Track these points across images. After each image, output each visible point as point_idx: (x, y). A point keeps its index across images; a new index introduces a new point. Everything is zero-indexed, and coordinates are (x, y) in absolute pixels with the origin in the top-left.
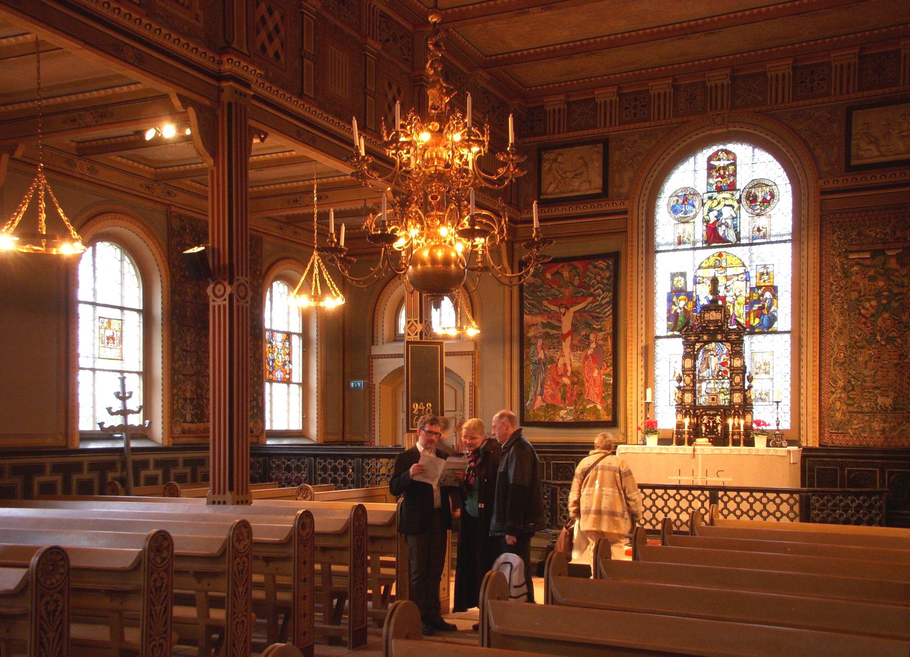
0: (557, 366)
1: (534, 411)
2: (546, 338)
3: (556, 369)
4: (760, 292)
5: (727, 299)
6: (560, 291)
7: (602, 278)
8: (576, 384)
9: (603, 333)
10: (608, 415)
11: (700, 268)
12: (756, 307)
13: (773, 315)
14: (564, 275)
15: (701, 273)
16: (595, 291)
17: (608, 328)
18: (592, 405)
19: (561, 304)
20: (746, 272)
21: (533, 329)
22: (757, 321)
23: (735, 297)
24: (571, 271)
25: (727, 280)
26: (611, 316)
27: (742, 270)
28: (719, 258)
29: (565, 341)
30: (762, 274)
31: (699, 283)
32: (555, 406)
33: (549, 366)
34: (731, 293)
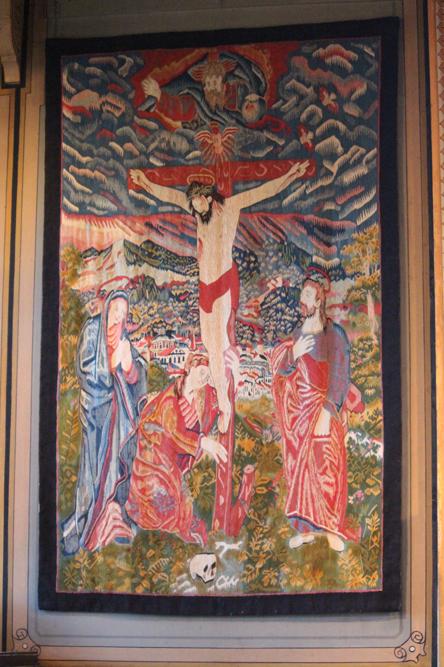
0: (179, 396)
1: (92, 557)
2: (142, 296)
3: (177, 407)
6: (190, 141)
7: (341, 101)
8: (252, 460)
9: (349, 283)
10: (368, 572)
14: (208, 88)
16: (315, 141)
17: (365, 269)
18: (310, 538)
19: (196, 184)
21: (92, 265)
24: (231, 74)
26: (376, 227)
29: (209, 310)
32: (171, 538)
33: (151, 398)
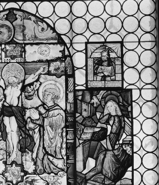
4: (95, 100)
5: (28, 114)
12: (87, 134)
13: (124, 151)
20: (65, 57)
22: (91, 163)
23: (43, 111)
27: (55, 51)
28: (8, 23)
30: (99, 62)
34: (36, 102)
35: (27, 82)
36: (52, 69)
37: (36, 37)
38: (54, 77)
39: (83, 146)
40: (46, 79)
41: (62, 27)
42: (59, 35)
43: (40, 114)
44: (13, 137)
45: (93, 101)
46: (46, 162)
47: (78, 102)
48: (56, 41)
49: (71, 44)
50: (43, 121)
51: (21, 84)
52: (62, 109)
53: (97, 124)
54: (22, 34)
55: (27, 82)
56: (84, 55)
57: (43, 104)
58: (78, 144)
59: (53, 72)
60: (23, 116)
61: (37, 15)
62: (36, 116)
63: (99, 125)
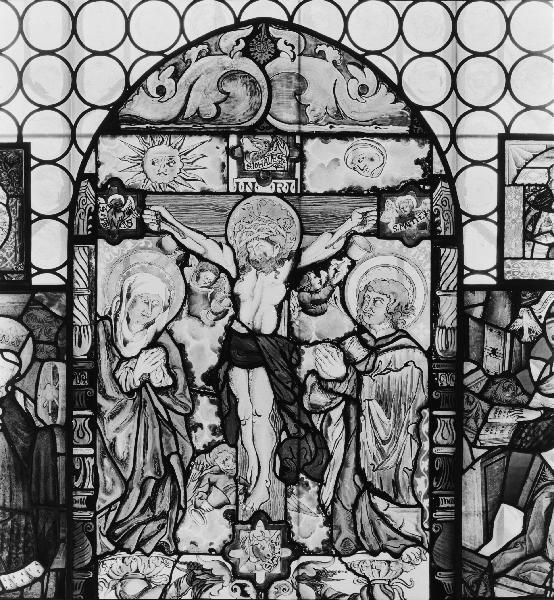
4: (526, 321)
5: (309, 359)
11: (116, 123)
12: (501, 426)
15: (117, 157)
20: (432, 181)
22: (510, 520)
23: (357, 351)
25: (308, 228)
27: (401, 161)
31: (115, 238)
34: (335, 322)
35: (307, 259)
36: (390, 216)
37: (339, 114)
38: (398, 243)
39: (484, 468)
40: (370, 249)
41: (425, 84)
42: (415, 110)
43: (349, 361)
44: (261, 435)
45: (518, 324)
46: (364, 514)
47: (472, 324)
48: (404, 129)
49: (454, 138)
50: (359, 385)
51: (288, 265)
52: (420, 348)
53: (531, 397)
54: (293, 103)
55: (307, 259)
56: (495, 176)
57: (360, 330)
58: (467, 459)
59: (392, 226)
60: (293, 366)
61: (346, 42)
62: (334, 367)
63: (538, 400)
